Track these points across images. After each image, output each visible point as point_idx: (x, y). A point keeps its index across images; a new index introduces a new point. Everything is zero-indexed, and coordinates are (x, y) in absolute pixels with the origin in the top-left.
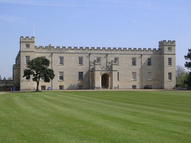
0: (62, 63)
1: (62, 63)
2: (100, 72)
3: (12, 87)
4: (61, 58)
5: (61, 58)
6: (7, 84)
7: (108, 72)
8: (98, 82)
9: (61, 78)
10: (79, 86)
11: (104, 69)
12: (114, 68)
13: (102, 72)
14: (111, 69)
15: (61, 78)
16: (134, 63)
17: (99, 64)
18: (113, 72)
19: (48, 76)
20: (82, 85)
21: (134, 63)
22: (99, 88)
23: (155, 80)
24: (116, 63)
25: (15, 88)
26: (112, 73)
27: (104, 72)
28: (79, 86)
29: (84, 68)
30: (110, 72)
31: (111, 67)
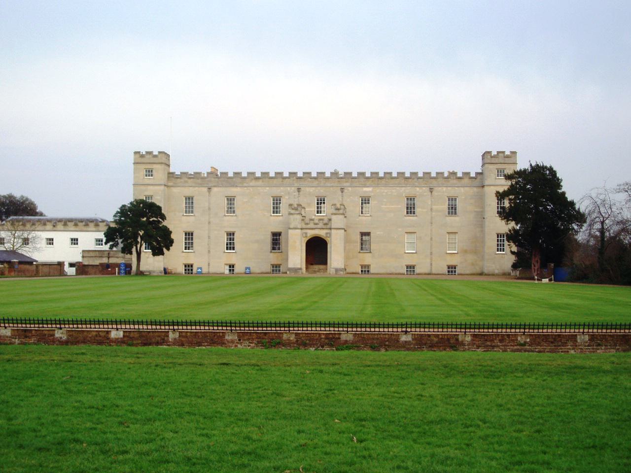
0: (231, 209)
1: (231, 209)
2: (299, 231)
3: (118, 265)
4: (231, 200)
5: (231, 200)
6: (110, 259)
7: (322, 233)
8: (296, 257)
9: (230, 246)
10: (273, 266)
11: (311, 225)
12: (338, 221)
13: (306, 233)
14: (327, 224)
15: (230, 246)
16: (411, 210)
17: (297, 212)
18: (333, 231)
19: (161, 241)
20: (279, 263)
21: (411, 210)
22: (296, 270)
23: (465, 252)
24: (341, 211)
25: (124, 267)
26: (330, 234)
27: (311, 233)
28: (273, 266)
29: (275, 223)
30: (327, 233)
31: (330, 220)
